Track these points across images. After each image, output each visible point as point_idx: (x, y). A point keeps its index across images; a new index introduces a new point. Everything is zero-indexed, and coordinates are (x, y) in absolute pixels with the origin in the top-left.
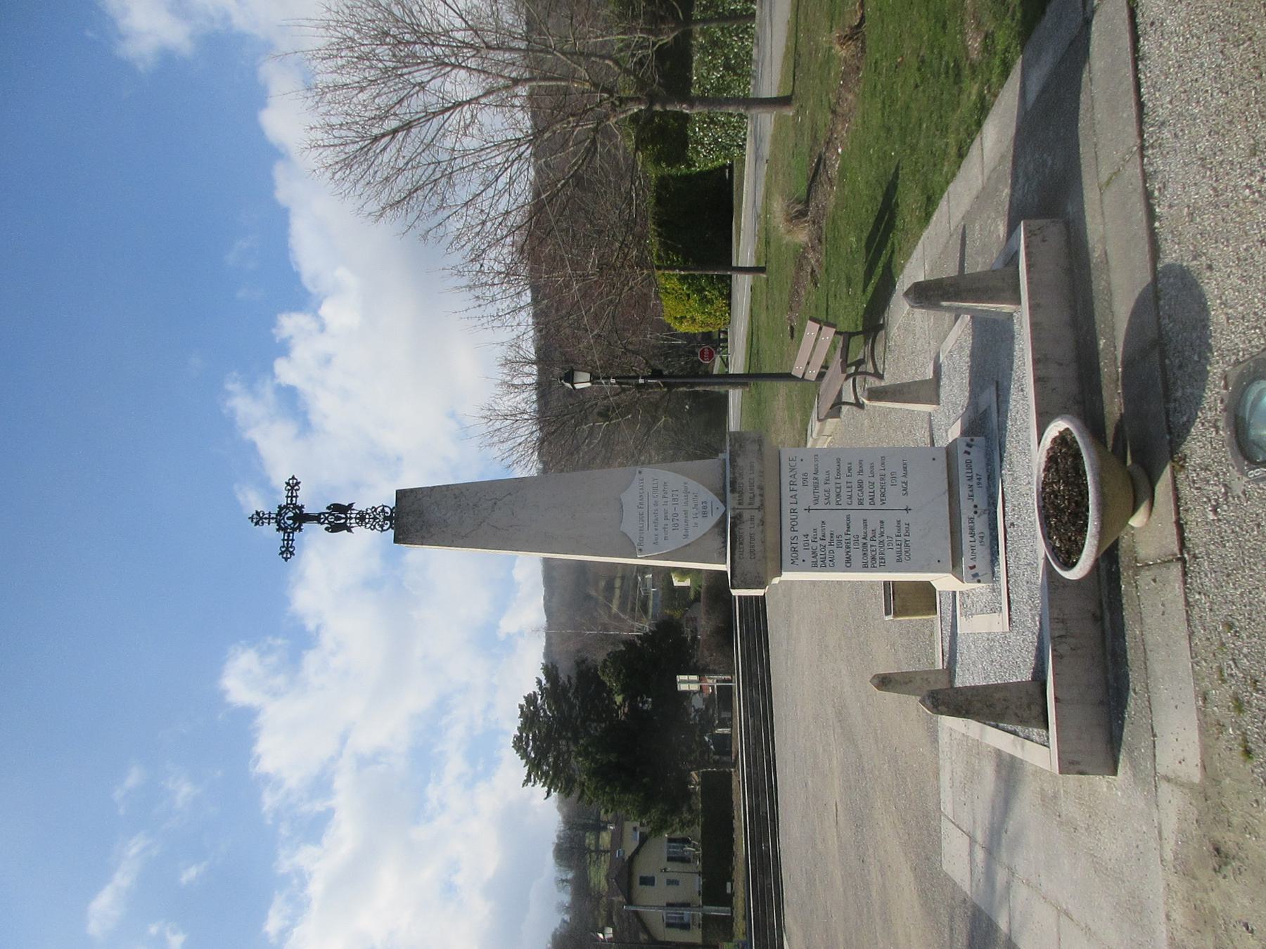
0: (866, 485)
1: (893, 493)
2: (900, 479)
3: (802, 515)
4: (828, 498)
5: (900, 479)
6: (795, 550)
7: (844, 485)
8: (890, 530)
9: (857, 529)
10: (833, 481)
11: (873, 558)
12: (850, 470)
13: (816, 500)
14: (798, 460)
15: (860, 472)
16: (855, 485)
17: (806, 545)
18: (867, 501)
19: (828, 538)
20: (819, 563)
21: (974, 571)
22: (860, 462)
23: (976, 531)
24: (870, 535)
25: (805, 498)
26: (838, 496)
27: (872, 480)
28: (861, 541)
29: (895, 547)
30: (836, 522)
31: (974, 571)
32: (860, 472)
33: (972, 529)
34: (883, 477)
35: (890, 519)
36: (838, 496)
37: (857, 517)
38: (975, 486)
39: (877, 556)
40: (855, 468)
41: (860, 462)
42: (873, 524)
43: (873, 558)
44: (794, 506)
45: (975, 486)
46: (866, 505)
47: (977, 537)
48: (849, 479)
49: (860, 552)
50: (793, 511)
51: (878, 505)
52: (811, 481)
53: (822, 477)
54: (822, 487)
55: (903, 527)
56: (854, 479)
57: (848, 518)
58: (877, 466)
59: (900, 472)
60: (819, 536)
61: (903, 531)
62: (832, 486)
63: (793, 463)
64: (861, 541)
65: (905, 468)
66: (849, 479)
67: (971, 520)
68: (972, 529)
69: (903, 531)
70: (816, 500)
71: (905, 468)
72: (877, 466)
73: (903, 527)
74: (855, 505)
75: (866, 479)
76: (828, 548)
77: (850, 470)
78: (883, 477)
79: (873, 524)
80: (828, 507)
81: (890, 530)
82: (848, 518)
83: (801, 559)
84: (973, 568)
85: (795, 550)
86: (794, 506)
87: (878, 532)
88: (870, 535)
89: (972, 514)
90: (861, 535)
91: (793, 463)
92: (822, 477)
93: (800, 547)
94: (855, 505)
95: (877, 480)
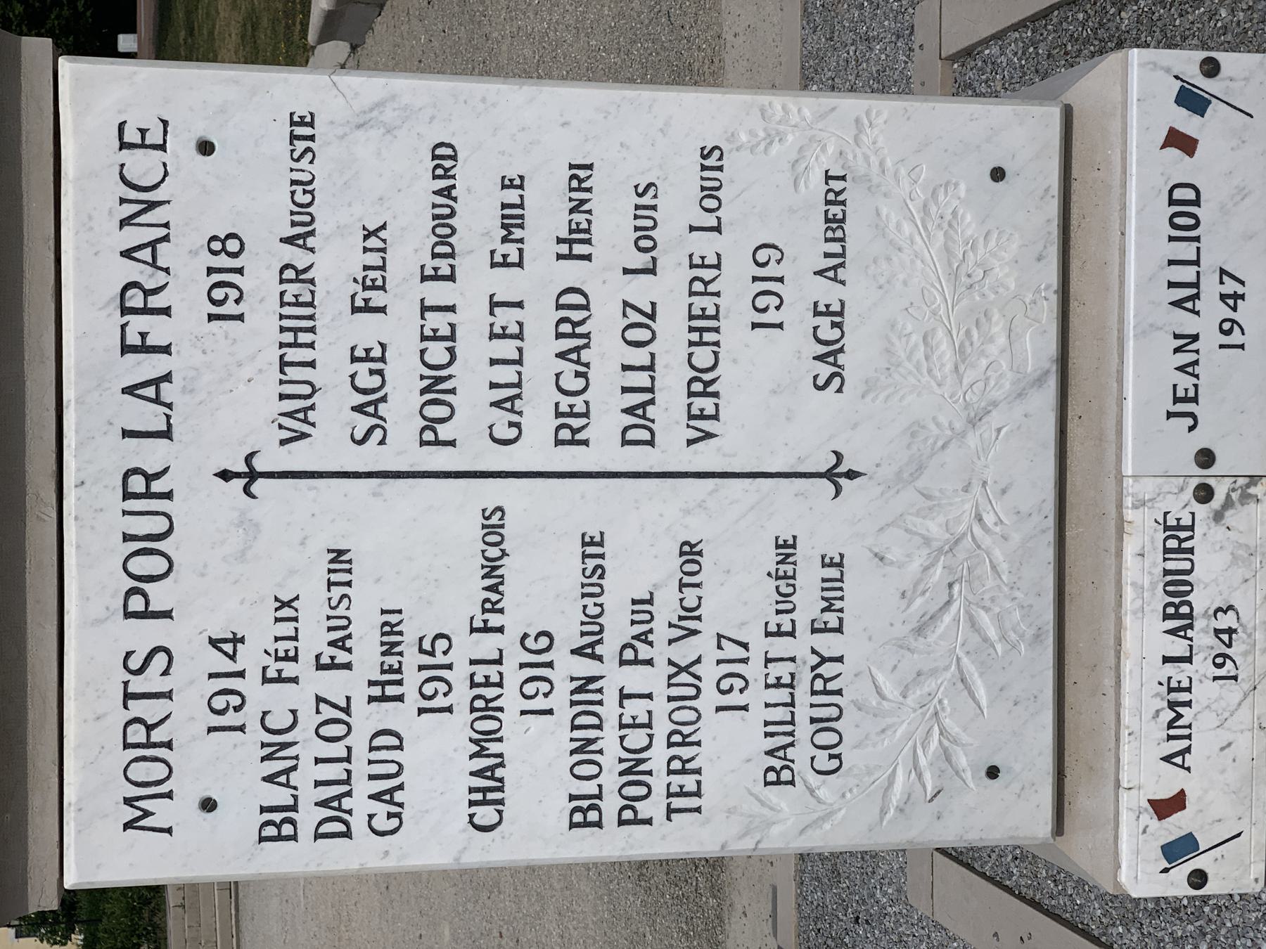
0: (605, 323)
1: (762, 369)
2: (803, 289)
3: (201, 509)
4: (370, 404)
5: (803, 289)
6: (146, 742)
7: (472, 322)
8: (736, 598)
9: (543, 594)
10: (403, 293)
11: (634, 768)
12: (512, 220)
13: (298, 420)
14: (181, 147)
15: (575, 244)
16: (540, 321)
17: (225, 706)
18: (607, 421)
19: (366, 652)
20: (308, 816)
21: (1177, 825)
22: (580, 176)
23: (1201, 601)
24: (618, 628)
25: (228, 388)
26: (436, 386)
27: (641, 291)
28: (566, 667)
29: (757, 696)
30: (415, 553)
31: (1177, 825)
32: (575, 244)
33: (1177, 587)
34: (704, 275)
35: (737, 533)
36: (436, 386)
37: (547, 524)
38: (1210, 339)
39: (658, 756)
40: (547, 217)
41: (580, 176)
42: (639, 568)
43: (634, 768)
44: (151, 455)
45: (1210, 339)
46: (604, 448)
47: (1202, 637)
48: (506, 284)
49: (555, 737)
50: (143, 487)
51: (672, 449)
52: (260, 278)
53: (335, 264)
54: (338, 333)
55: (809, 577)
56: (543, 276)
57: (493, 525)
58: (678, 207)
59: (806, 246)
60: (314, 640)
61: (808, 604)
62: (398, 330)
63: (143, 166)
64: (566, 667)
65: (835, 223)
66: (506, 284)
67: (1178, 538)
68: (1177, 587)
69: (808, 604)
70: (298, 420)
71: (835, 223)
72: (678, 207)
73: (809, 577)
74: (537, 448)
75: (608, 293)
76: (367, 719)
77: (512, 220)
78: (704, 275)
79: (639, 568)
80: (369, 457)
81: (736, 598)
82: (493, 525)
83: (188, 789)
84: (1166, 807)
85: (146, 742)
86: (151, 455)
87: (666, 609)
88: (618, 628)
89: (1181, 506)
90: (569, 632)
91: (143, 166)
92: (335, 264)
93: (187, 716)
94: (537, 448)
95: (669, 291)
